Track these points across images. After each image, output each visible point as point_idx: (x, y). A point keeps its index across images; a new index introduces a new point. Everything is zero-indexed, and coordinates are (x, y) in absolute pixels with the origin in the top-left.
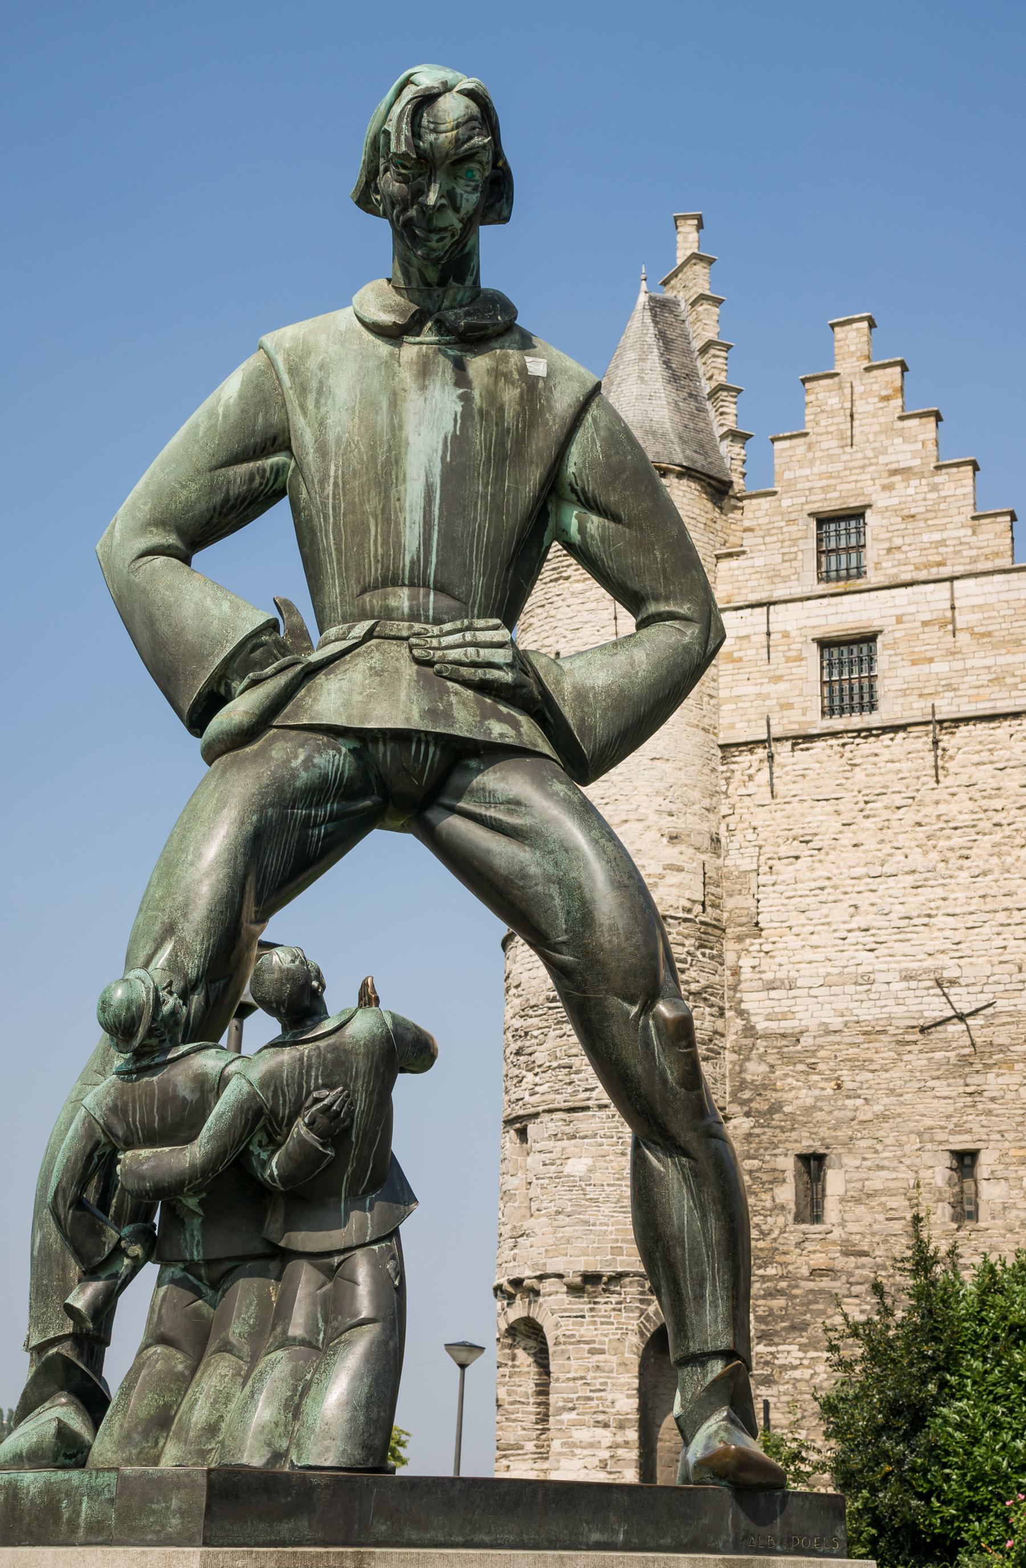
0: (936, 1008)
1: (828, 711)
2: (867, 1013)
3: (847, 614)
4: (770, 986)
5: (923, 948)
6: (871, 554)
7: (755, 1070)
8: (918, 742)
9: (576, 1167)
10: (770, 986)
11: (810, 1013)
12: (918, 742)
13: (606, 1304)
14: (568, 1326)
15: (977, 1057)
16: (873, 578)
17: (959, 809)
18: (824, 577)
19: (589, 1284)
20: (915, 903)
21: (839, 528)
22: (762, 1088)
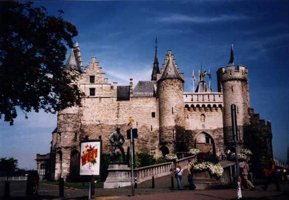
0: (98, 123)
1: (91, 95)
2: (93, 123)
3: (93, 86)
4: (84, 120)
5: (98, 118)
6: (95, 80)
7: (82, 128)
8: (98, 99)
9: (66, 137)
10: (84, 120)
11: (87, 123)
12: (98, 99)
13: (68, 149)
14: (64, 151)
15: (102, 128)
16: (95, 83)
17: (102, 105)
18: (91, 82)
19: (66, 148)
20: (97, 114)
21: (92, 79)
22: (83, 130)
